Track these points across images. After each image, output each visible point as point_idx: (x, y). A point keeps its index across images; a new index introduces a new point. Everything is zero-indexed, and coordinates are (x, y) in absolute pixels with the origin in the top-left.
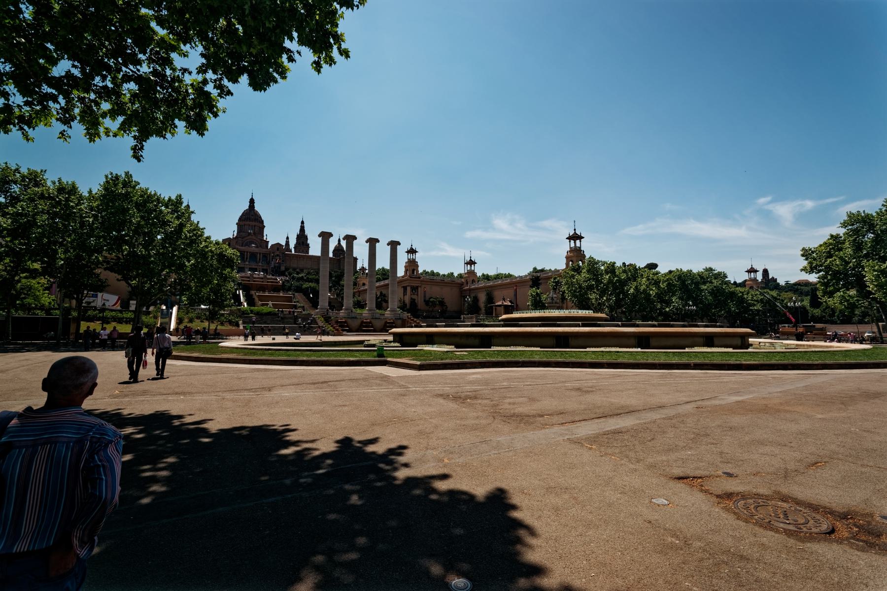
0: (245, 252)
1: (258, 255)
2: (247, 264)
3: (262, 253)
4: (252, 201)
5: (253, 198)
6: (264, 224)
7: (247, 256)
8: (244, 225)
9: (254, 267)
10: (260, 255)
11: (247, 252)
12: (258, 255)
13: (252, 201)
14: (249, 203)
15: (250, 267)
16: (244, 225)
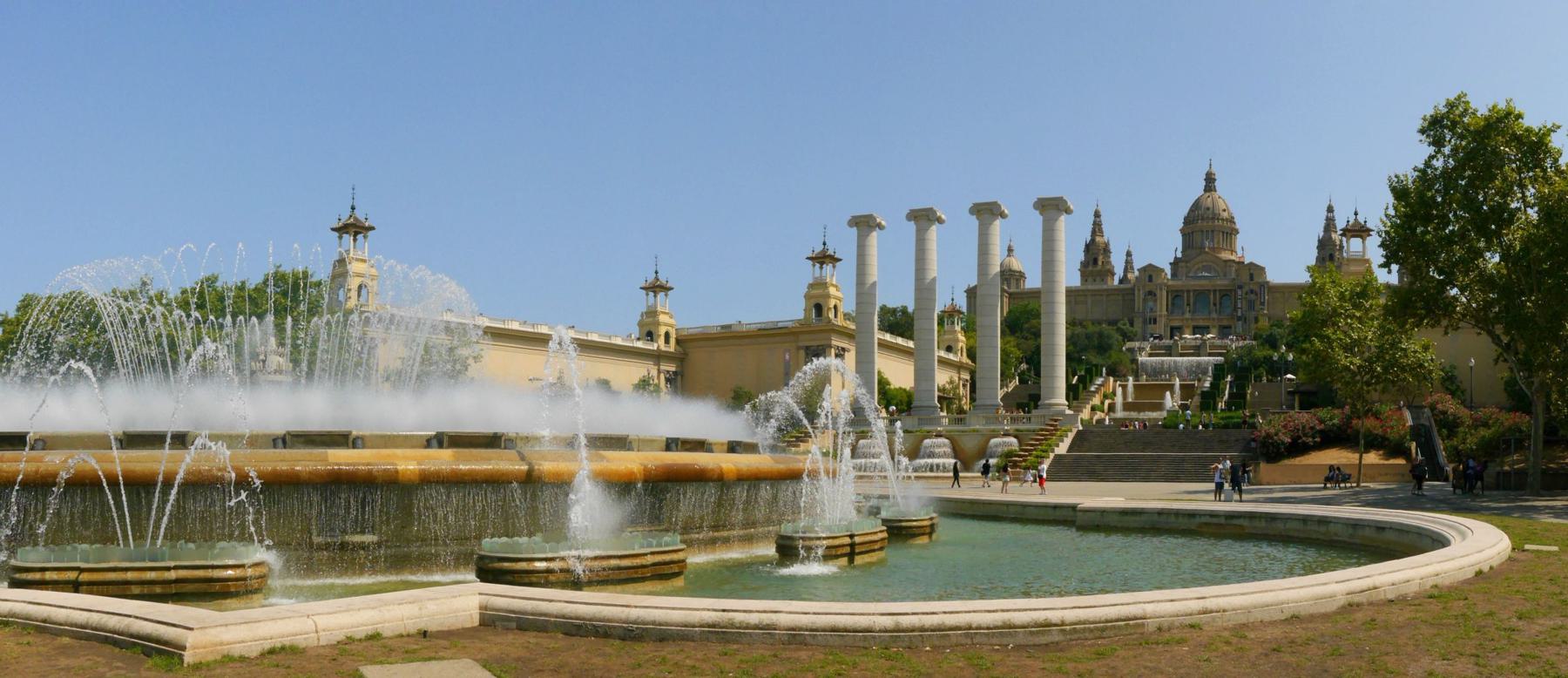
0: (1181, 291)
1: (1212, 296)
2: (1187, 320)
3: (1220, 290)
4: (1210, 181)
5: (1214, 170)
6: (1238, 226)
7: (1188, 300)
8: (1192, 233)
9: (1201, 323)
10: (1215, 295)
11: (1188, 291)
12: (1212, 296)
13: (1210, 181)
15: (1195, 324)
16: (1192, 233)
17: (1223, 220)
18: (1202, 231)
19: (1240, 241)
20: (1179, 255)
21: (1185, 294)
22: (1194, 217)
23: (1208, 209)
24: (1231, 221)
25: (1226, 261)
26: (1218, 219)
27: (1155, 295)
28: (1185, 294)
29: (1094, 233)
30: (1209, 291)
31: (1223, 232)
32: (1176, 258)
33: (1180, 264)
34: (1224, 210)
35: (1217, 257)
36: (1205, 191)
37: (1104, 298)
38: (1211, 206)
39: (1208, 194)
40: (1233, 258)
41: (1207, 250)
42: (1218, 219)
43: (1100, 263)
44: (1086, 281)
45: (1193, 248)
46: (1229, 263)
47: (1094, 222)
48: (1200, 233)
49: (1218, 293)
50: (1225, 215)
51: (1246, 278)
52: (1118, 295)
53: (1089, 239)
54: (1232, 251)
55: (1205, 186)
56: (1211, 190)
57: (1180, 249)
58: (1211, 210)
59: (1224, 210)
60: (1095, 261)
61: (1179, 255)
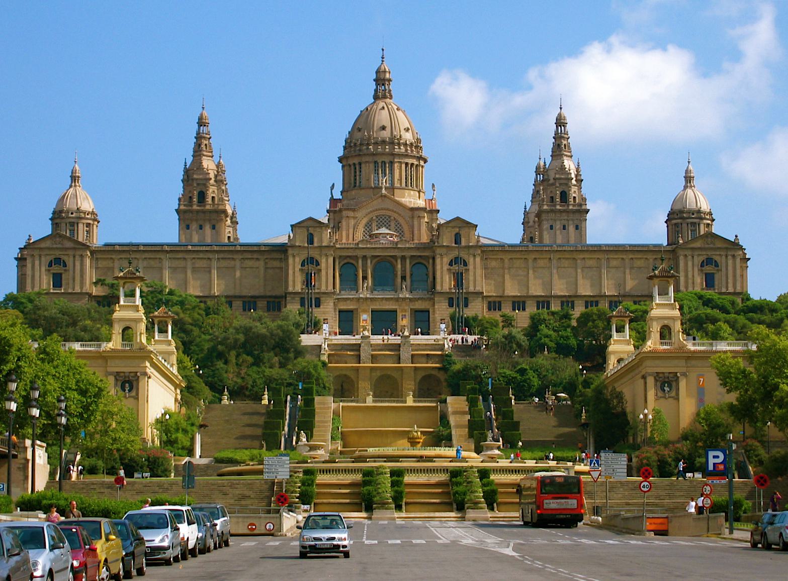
1: (399, 266)
3: (412, 257)
7: (365, 271)
14: (373, 85)
15: (377, 306)
16: (360, 164)
17: (405, 144)
18: (376, 162)
19: (427, 174)
20: (337, 195)
21: (360, 262)
22: (362, 139)
23: (384, 128)
24: (417, 147)
25: (413, 210)
26: (399, 144)
27: (318, 264)
28: (360, 262)
29: (198, 152)
30: (394, 257)
31: (407, 164)
32: (333, 201)
33: (345, 213)
34: (407, 130)
35: (399, 204)
36: (376, 97)
37: (238, 263)
38: (387, 124)
39: (381, 104)
40: (421, 203)
41: (384, 191)
42: (399, 144)
43: (209, 200)
44: (188, 227)
45: (360, 188)
46: (416, 212)
47: (198, 133)
48: (372, 166)
49: (408, 261)
50: (408, 137)
51: (447, 240)
52: (258, 259)
53: (190, 160)
54: (419, 192)
55: (376, 91)
56: (385, 97)
57: (339, 187)
58: (388, 129)
59: (407, 130)
60: (202, 196)
61: (337, 195)
